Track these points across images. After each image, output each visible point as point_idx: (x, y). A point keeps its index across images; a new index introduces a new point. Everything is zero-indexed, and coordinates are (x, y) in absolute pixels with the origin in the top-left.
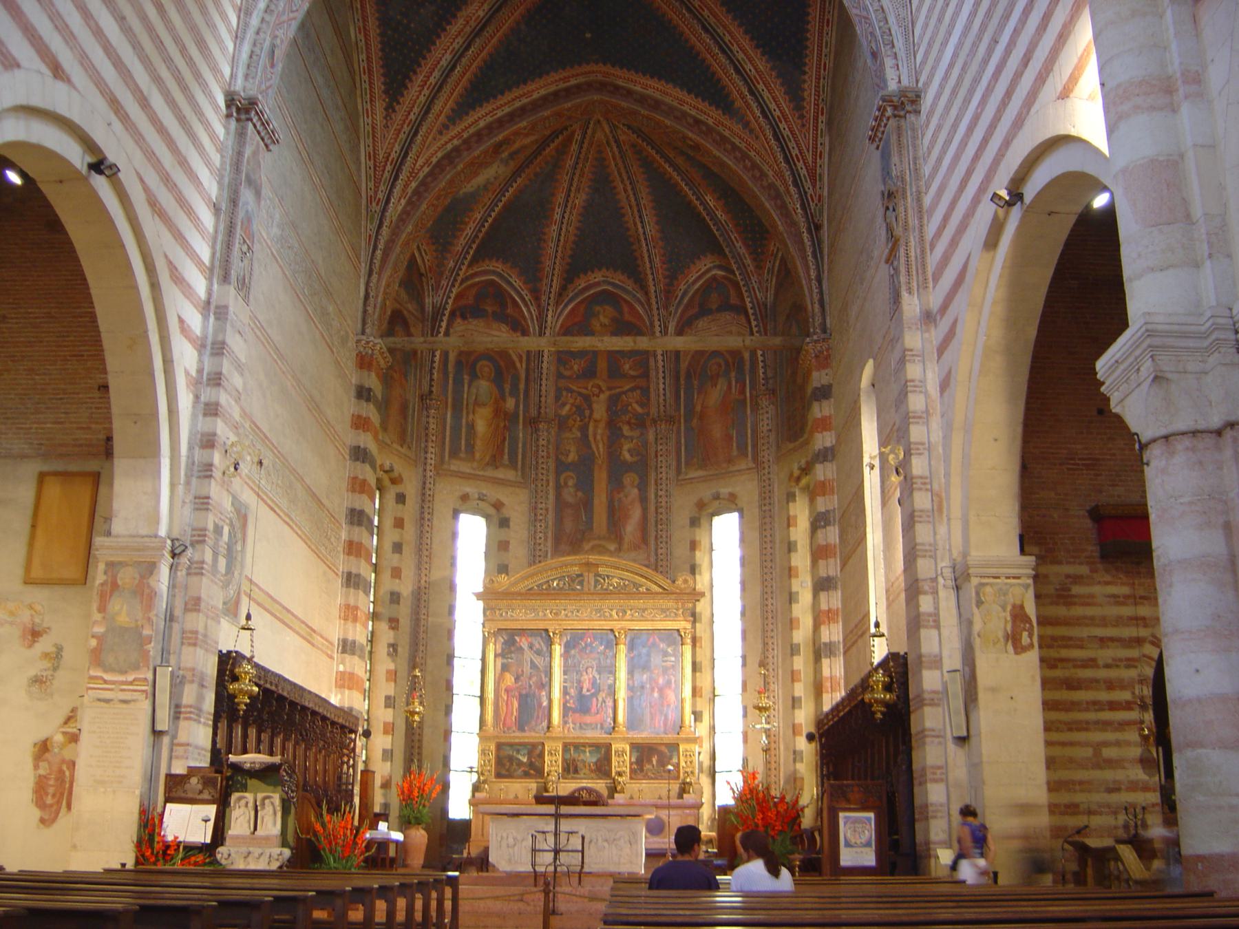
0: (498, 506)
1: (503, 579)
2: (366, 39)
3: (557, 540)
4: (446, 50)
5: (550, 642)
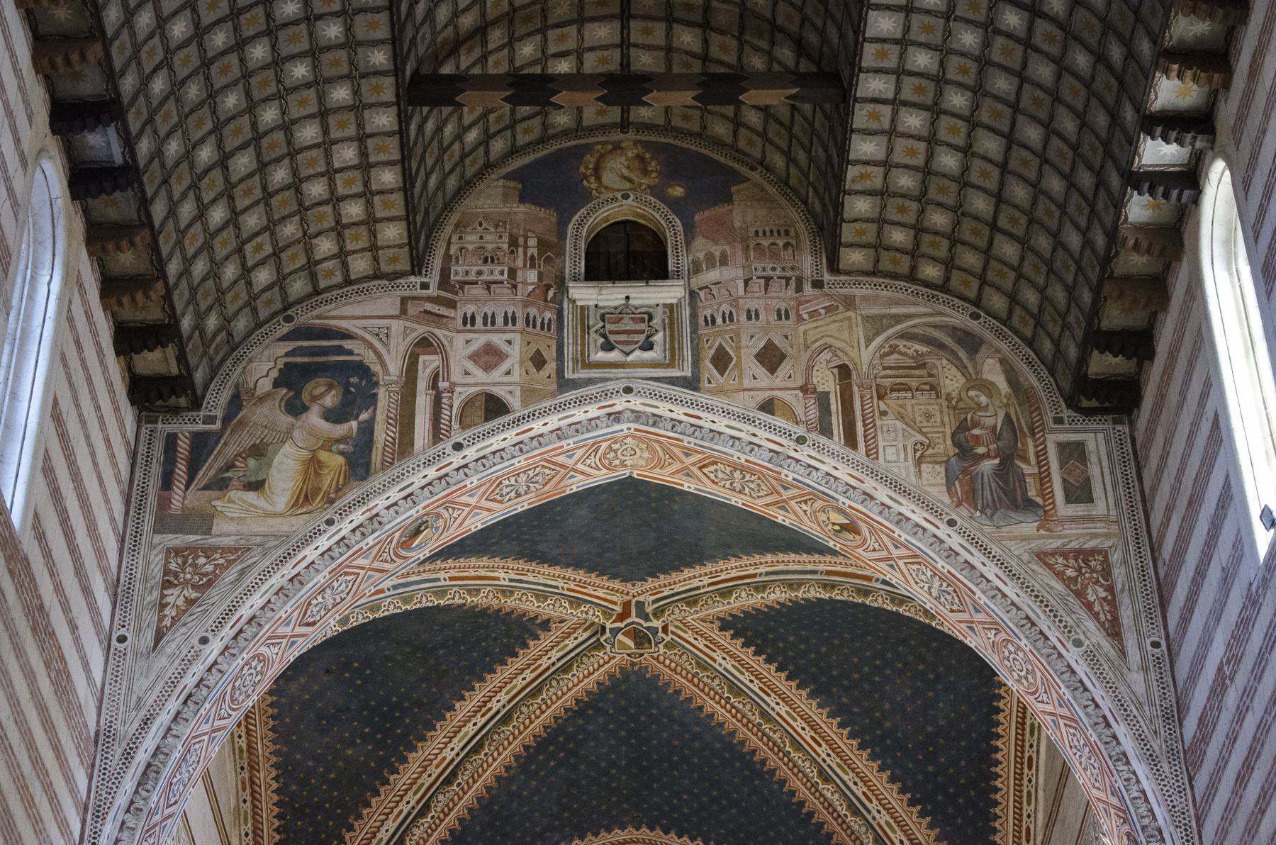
2: (254, 798)
4: (387, 814)
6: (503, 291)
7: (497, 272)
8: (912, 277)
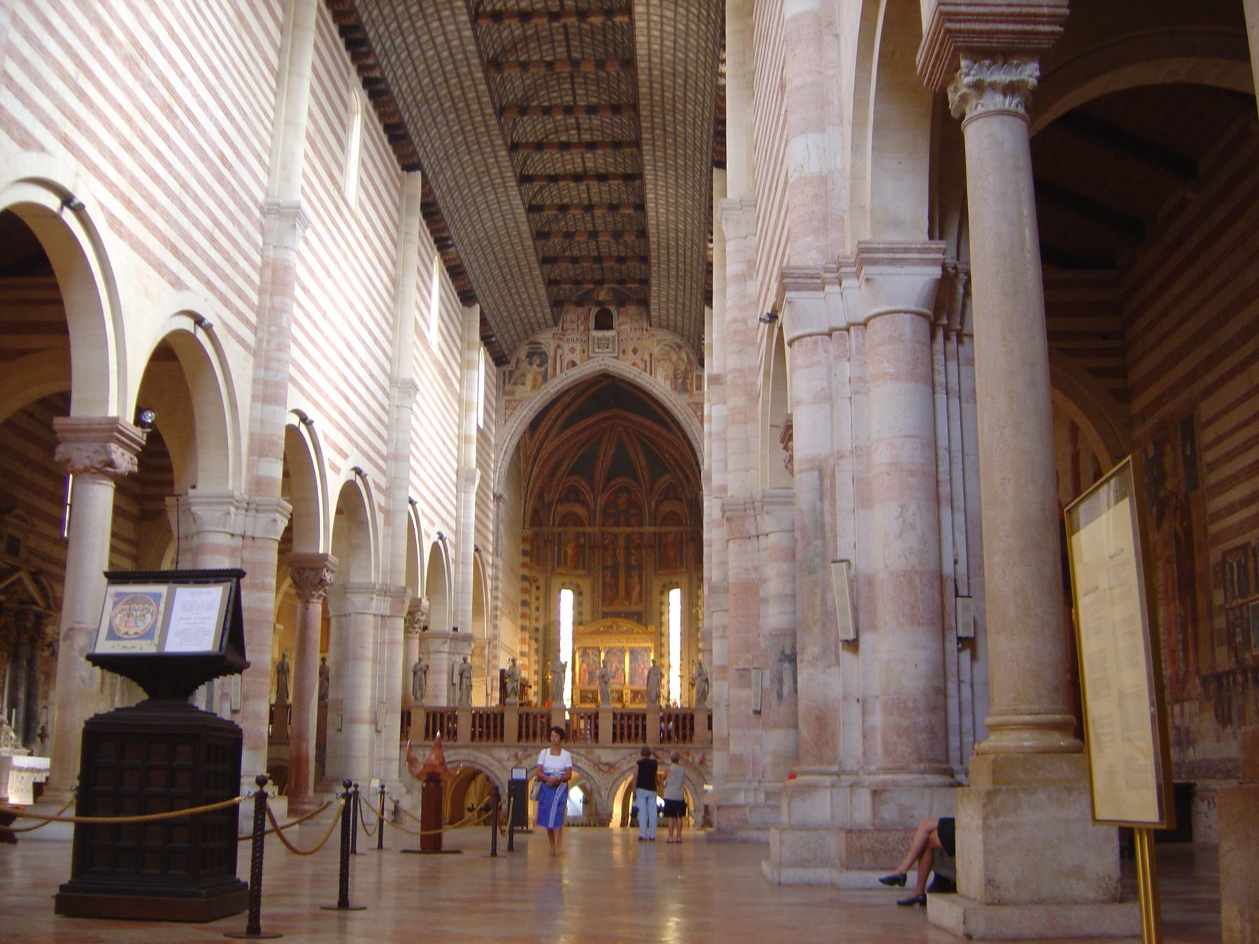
0: (578, 586)
1: (582, 628)
3: (603, 600)
5: (600, 652)
6: (576, 331)
7: (575, 326)
8: (668, 329)
